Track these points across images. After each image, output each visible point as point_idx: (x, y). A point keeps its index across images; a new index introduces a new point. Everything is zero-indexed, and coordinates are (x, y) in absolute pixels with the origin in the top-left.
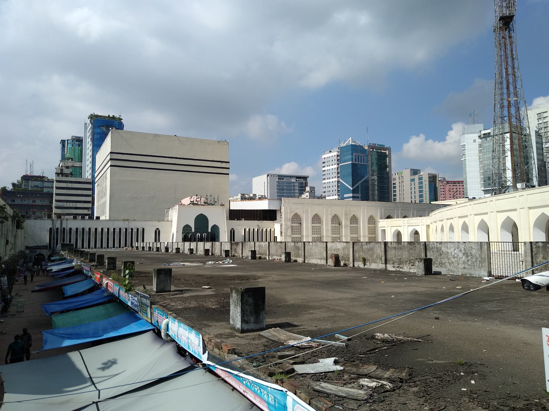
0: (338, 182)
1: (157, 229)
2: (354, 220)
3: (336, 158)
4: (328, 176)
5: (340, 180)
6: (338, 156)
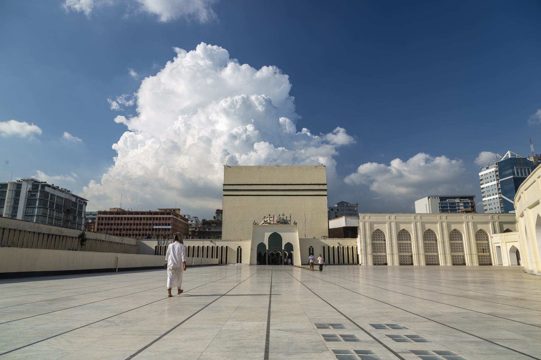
0: (500, 198)
1: (239, 247)
2: (455, 235)
5: (503, 196)
6: (496, 171)
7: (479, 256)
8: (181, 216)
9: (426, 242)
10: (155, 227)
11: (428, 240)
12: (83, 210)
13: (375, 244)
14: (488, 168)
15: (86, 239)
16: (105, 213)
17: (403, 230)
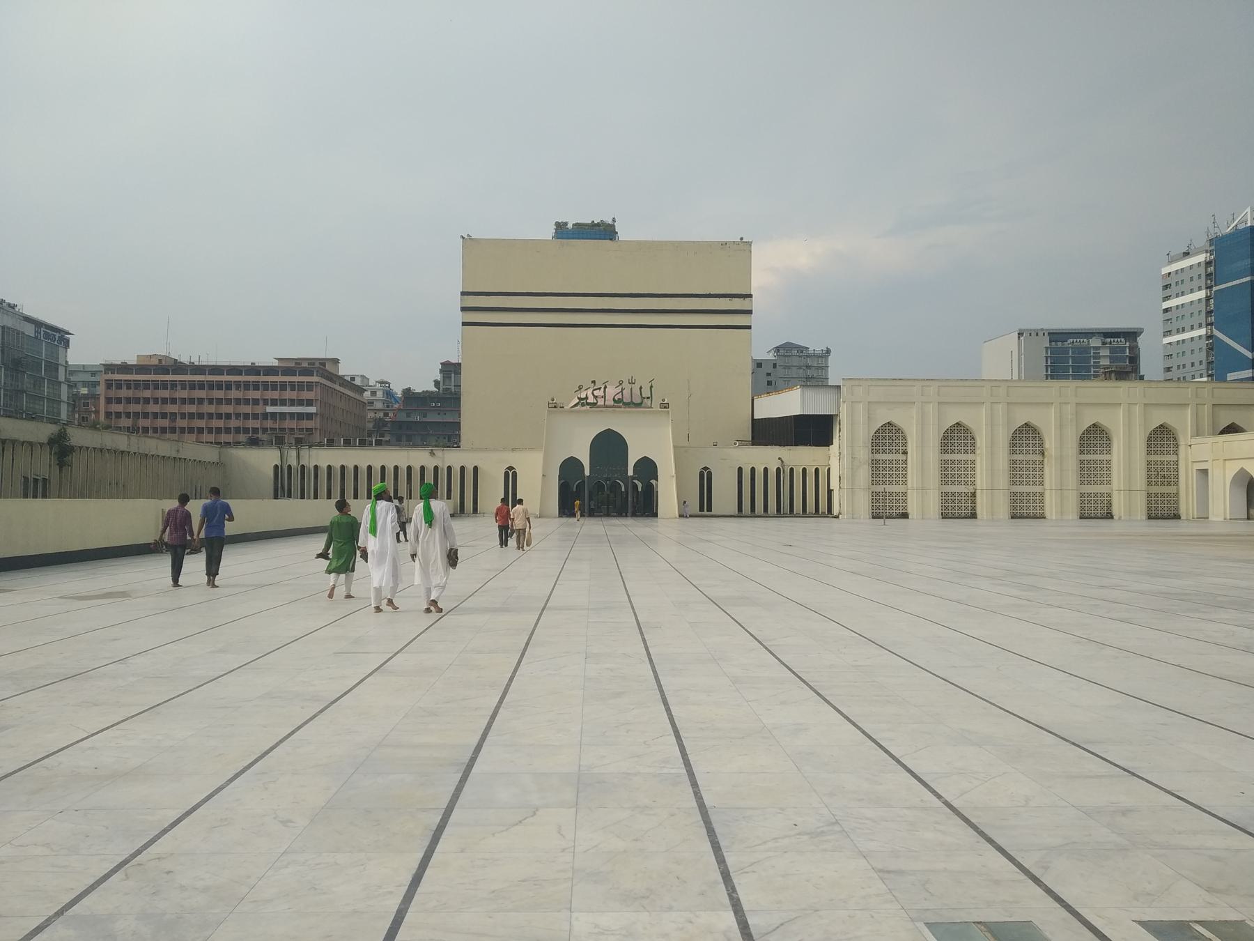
1: (511, 468)
2: (1095, 438)
3: (1202, 271)
4: (1180, 325)
6: (1208, 264)
7: (1149, 495)
8: (341, 378)
9: (1016, 457)
10: (270, 409)
11: (1021, 452)
12: (61, 361)
13: (877, 461)
14: (1186, 254)
15: (72, 449)
16: (124, 368)
17: (958, 424)
